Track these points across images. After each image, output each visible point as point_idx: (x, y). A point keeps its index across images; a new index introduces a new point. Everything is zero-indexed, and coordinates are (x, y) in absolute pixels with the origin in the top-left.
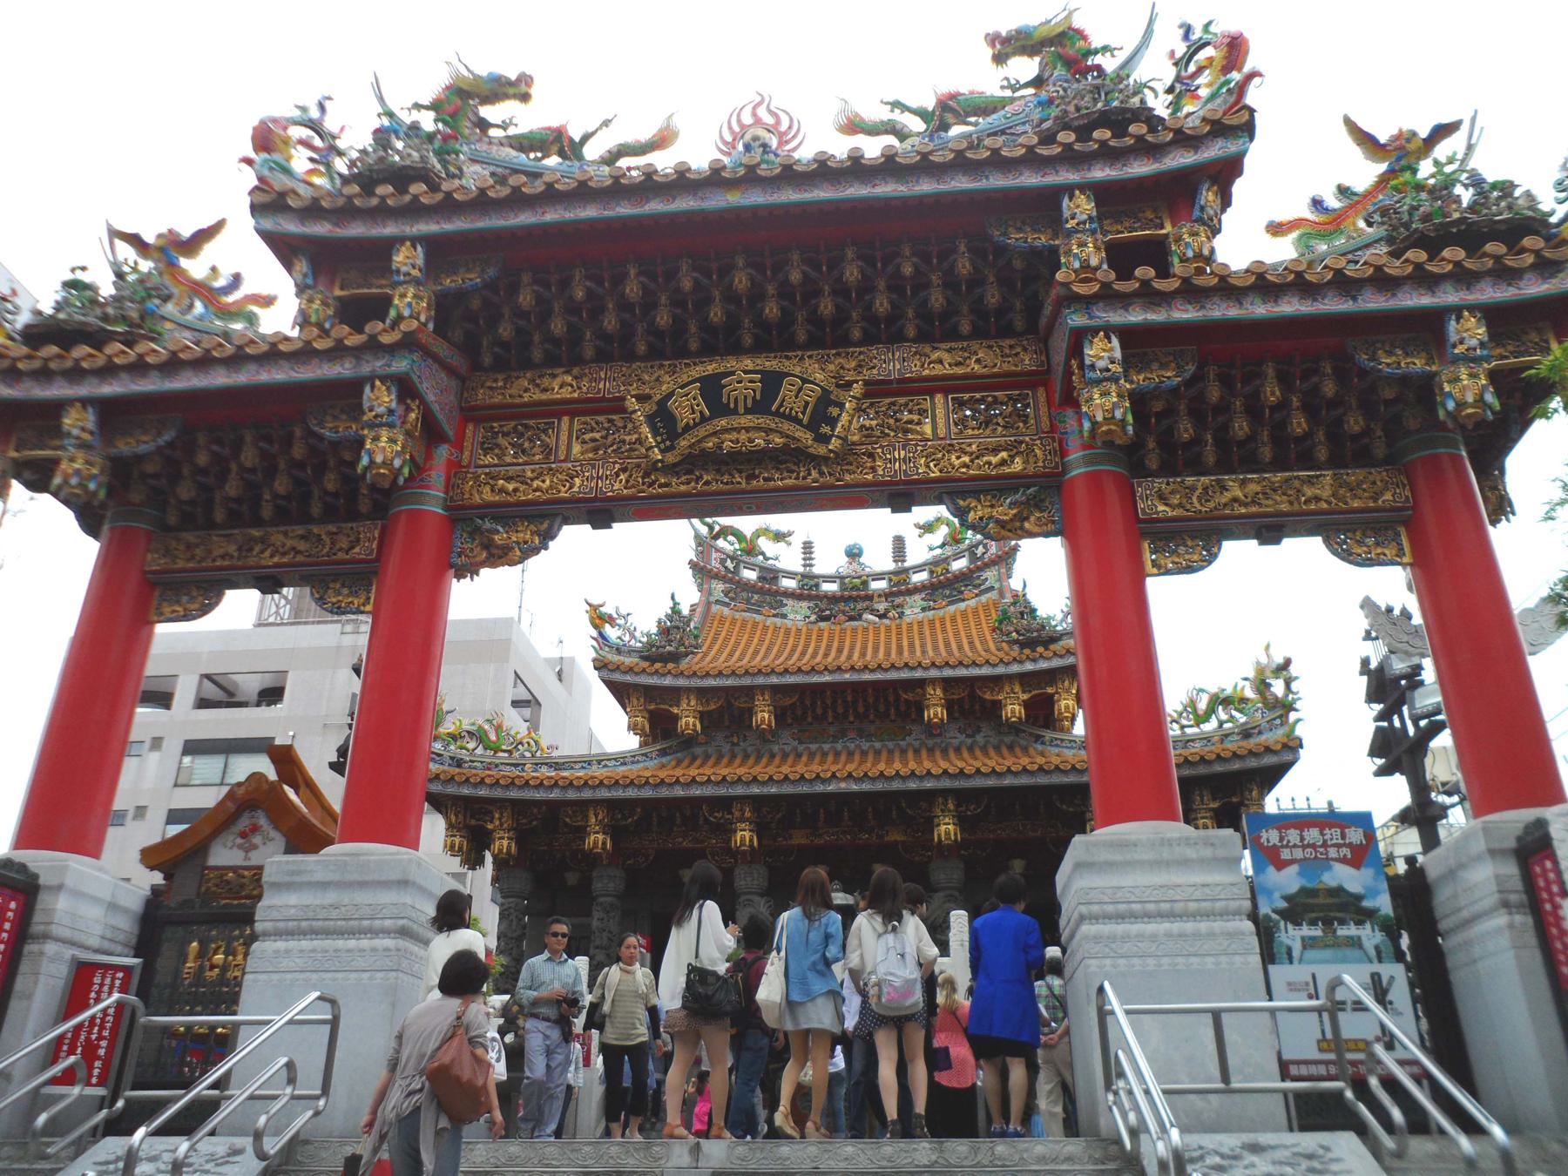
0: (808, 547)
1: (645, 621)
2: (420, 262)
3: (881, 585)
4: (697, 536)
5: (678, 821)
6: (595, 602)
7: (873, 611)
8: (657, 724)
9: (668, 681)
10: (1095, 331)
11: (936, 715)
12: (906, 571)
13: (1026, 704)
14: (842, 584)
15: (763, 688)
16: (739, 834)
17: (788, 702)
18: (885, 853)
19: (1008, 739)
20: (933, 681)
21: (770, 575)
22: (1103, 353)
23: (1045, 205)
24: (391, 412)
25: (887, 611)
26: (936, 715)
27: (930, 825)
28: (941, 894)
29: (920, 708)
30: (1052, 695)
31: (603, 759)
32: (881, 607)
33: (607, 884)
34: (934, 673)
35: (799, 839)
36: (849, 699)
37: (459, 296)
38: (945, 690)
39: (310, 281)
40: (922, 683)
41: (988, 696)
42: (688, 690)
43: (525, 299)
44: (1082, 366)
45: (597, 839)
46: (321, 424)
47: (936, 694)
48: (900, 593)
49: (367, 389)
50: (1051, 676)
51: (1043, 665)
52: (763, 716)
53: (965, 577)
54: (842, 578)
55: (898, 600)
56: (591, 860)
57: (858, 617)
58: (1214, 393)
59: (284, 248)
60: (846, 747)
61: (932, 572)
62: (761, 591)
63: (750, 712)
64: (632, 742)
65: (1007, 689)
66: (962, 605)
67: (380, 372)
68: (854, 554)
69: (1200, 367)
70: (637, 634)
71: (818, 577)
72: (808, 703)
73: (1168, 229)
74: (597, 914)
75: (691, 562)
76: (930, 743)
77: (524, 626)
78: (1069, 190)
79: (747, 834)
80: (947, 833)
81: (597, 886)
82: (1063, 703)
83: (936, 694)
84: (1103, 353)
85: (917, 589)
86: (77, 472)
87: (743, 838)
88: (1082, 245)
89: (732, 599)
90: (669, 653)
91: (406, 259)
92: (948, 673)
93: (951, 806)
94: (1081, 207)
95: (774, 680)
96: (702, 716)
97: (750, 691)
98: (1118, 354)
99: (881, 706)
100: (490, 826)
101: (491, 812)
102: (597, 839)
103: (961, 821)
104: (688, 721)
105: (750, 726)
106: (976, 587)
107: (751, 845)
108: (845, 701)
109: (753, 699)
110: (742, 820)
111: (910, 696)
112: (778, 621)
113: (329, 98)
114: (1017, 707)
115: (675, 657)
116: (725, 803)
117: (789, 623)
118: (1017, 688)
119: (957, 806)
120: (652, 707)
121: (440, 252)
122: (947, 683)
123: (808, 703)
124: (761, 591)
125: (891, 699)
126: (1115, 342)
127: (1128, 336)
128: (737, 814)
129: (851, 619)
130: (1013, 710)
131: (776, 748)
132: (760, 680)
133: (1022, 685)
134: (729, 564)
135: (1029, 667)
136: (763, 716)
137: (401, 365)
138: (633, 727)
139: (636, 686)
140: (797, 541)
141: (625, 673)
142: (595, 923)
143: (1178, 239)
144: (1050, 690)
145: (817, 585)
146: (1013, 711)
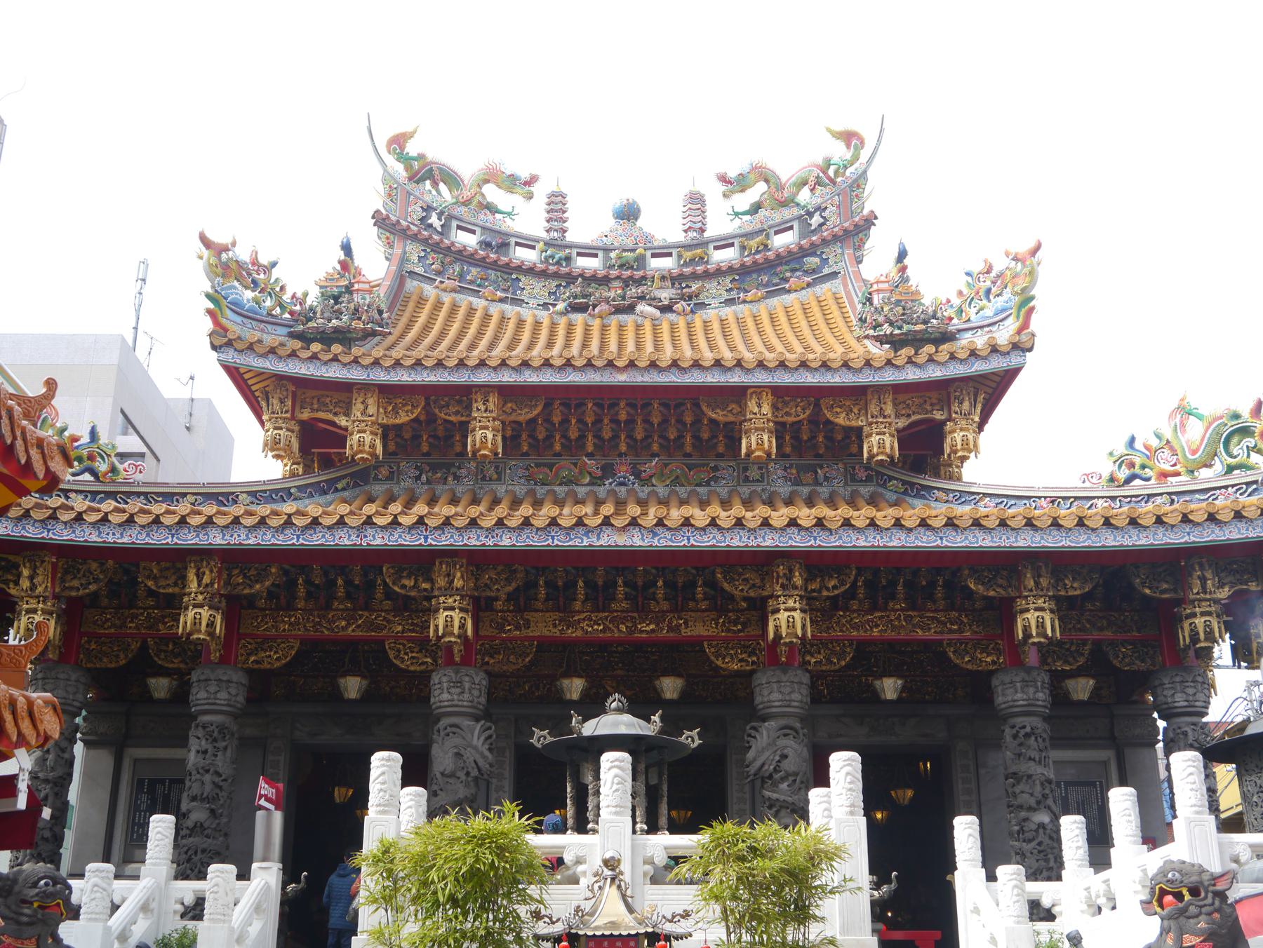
0: (557, 207)
1: (303, 277)
3: (667, 264)
4: (388, 177)
5: (341, 592)
6: (217, 237)
7: (652, 301)
8: (316, 446)
9: (333, 373)
11: (760, 444)
12: (704, 244)
13: (905, 437)
14: (607, 258)
15: (486, 389)
16: (442, 616)
17: (524, 415)
18: (678, 655)
19: (865, 490)
20: (759, 390)
21: (500, 242)
25: (673, 302)
26: (760, 444)
27: (761, 609)
28: (772, 724)
29: (732, 434)
30: (943, 423)
31: (223, 496)
32: (665, 295)
33: (216, 694)
34: (761, 378)
35: (543, 626)
36: (623, 416)
38: (775, 407)
40: (738, 394)
41: (841, 420)
42: (365, 387)
45: (199, 618)
47: (761, 410)
48: (695, 276)
50: (944, 391)
51: (935, 373)
52: (485, 435)
53: (793, 259)
54: (607, 250)
55: (695, 287)
56: (191, 652)
57: (630, 309)
60: (612, 493)
61: (743, 248)
62: (482, 263)
63: (464, 429)
64: (272, 470)
65: (873, 409)
66: (788, 299)
68: (628, 214)
70: (286, 297)
71: (570, 246)
72: (556, 419)
74: (194, 744)
75: (377, 215)
76: (745, 490)
77: (141, 353)
79: (456, 616)
80: (791, 624)
81: (199, 696)
82: (958, 436)
83: (761, 410)
85: (719, 273)
87: (448, 623)
89: (439, 273)
90: (336, 330)
92: (785, 379)
93: (798, 580)
95: (507, 377)
96: (387, 433)
97: (464, 394)
99: (680, 427)
100: (13, 592)
101: (17, 566)
102: (199, 618)
103: (818, 608)
104: (362, 439)
105: (463, 453)
106: (807, 272)
107: (463, 636)
108: (615, 421)
109: (469, 408)
110: (449, 590)
111: (719, 415)
112: (510, 309)
114: (888, 440)
115: (343, 337)
116: (421, 562)
117: (527, 314)
118: (889, 409)
119: (806, 581)
120: (305, 415)
122: (781, 394)
123: (556, 419)
124: (482, 263)
125: (688, 419)
128: (441, 582)
129: (619, 310)
130: (881, 442)
131: (501, 490)
132: (483, 377)
133: (895, 405)
134: (434, 220)
135: (912, 375)
136: (485, 435)
138: (273, 446)
139: (281, 378)
140: (541, 191)
141: (264, 356)
142: (192, 758)
144: (938, 416)
145: (568, 259)
146: (881, 445)
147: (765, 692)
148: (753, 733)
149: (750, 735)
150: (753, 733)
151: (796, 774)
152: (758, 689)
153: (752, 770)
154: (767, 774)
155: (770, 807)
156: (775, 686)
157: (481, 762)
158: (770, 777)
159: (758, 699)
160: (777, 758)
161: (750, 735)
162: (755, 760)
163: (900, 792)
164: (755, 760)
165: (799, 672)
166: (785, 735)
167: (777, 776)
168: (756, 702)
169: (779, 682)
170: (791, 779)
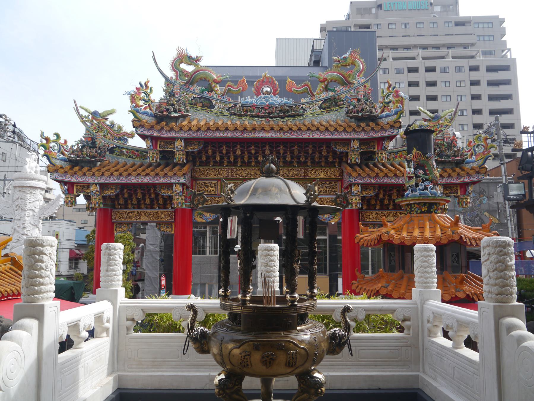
2: (183, 145)
10: (355, 184)
22: (356, 189)
23: (347, 142)
24: (180, 192)
37: (193, 152)
39: (152, 147)
43: (210, 152)
44: (351, 189)
46: (160, 191)
49: (174, 186)
58: (381, 196)
59: (144, 137)
67: (177, 182)
69: (379, 190)
73: (376, 150)
78: (354, 140)
84: (356, 189)
86: (97, 203)
88: (355, 154)
91: (179, 144)
94: (356, 145)
98: (360, 190)
113: (148, 82)
121: (188, 141)
126: (360, 186)
127: (362, 185)
137: (182, 180)
143: (378, 154)
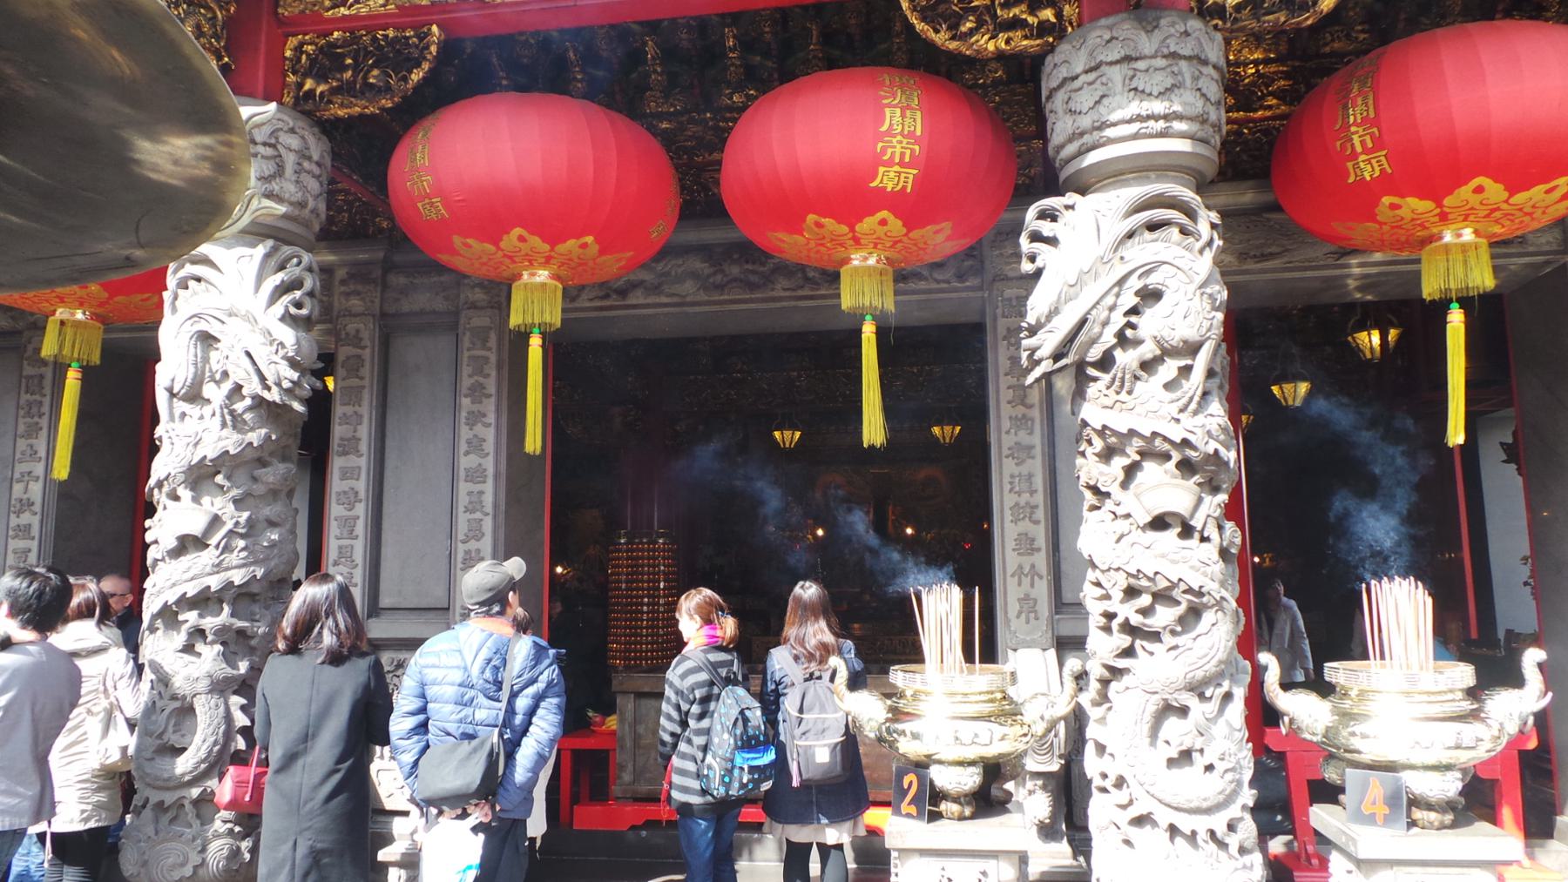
147: (1084, 100)
148: (1046, 228)
149: (1036, 237)
150: (1046, 228)
151: (1192, 349)
152: (1060, 96)
153: (1047, 342)
154: (1095, 354)
155: (1107, 455)
156: (1116, 74)
157: (263, 355)
158: (1106, 362)
159: (1060, 128)
160: (1129, 300)
161: (1036, 237)
162: (1054, 312)
163: (1288, 387)
164: (1054, 312)
165: (1195, 24)
166: (1153, 227)
167: (1126, 359)
168: (1056, 138)
169: (1128, 59)
170: (1169, 369)
